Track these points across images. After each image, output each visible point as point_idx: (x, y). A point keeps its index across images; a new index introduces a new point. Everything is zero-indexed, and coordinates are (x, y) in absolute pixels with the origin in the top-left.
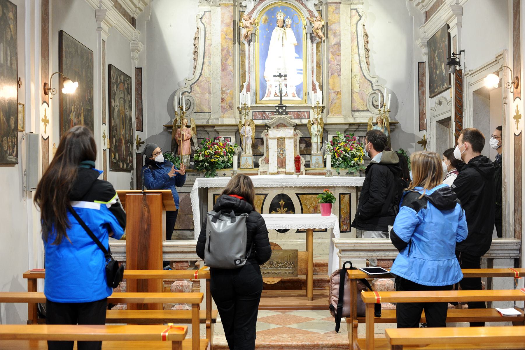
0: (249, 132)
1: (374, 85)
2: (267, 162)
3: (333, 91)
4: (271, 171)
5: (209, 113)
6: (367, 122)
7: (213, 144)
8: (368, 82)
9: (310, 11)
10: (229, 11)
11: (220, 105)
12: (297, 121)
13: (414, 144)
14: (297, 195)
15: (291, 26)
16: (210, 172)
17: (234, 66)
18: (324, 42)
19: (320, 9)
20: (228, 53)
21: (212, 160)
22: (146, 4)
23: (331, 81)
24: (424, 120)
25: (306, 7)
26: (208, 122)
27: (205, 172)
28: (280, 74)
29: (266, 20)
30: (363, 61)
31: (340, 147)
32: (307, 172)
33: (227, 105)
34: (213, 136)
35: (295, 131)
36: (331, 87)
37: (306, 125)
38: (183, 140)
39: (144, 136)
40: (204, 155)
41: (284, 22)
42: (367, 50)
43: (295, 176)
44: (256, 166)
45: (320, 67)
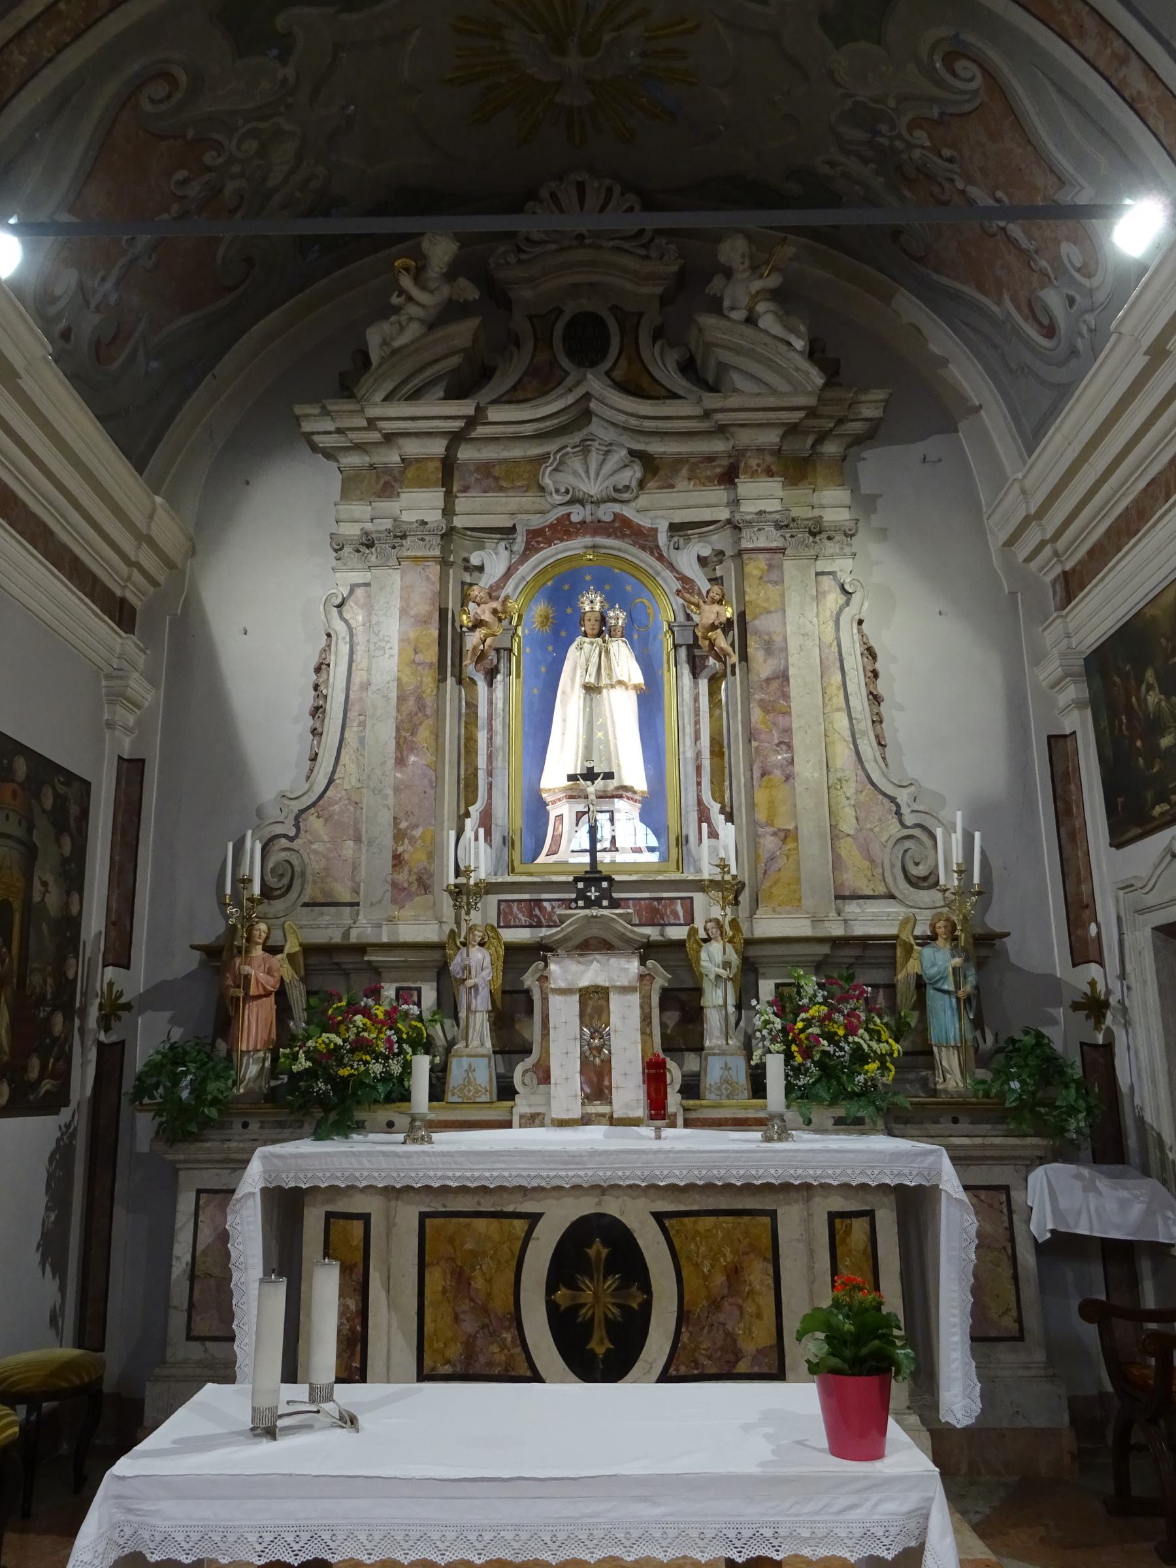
0: (480, 966)
1: (905, 810)
2: (544, 1075)
3: (769, 830)
5: (352, 904)
6: (894, 931)
8: (886, 801)
9: (684, 579)
10: (428, 578)
11: (389, 878)
12: (652, 933)
15: (626, 634)
18: (733, 673)
19: (718, 574)
20: (421, 707)
22: (170, 564)
23: (760, 796)
25: (671, 567)
26: (346, 934)
29: (547, 617)
30: (864, 733)
31: (808, 1023)
32: (693, 1115)
33: (413, 878)
35: (643, 963)
36: (761, 816)
37: (680, 944)
39: (133, 982)
41: (603, 620)
44: (506, 1091)
45: (721, 754)
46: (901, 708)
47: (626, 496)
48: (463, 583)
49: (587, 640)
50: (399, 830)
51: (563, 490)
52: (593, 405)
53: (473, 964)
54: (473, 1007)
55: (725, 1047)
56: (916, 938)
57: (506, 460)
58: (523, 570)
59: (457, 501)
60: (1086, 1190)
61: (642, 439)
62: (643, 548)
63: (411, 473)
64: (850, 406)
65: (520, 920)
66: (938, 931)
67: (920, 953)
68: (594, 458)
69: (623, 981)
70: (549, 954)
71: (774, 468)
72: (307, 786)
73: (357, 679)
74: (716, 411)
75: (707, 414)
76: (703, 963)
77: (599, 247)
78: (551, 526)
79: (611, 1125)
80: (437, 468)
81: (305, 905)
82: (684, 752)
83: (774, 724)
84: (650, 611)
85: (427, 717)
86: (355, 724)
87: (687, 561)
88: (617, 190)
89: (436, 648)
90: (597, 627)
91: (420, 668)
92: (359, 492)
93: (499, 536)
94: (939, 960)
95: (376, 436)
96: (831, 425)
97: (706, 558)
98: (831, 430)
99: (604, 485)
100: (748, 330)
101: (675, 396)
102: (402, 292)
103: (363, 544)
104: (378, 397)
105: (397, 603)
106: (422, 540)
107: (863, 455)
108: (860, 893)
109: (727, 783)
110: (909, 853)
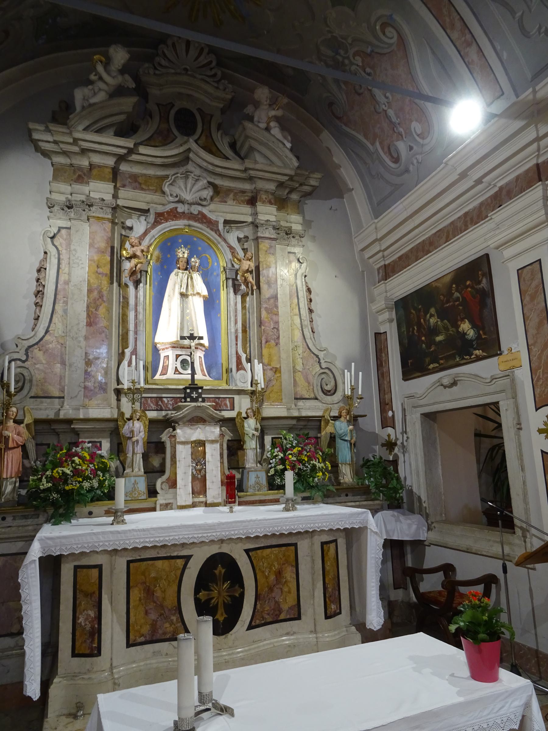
0: (138, 430)
2: (173, 484)
3: (269, 367)
4: (180, 502)
5: (59, 398)
6: (320, 414)
7: (70, 455)
8: (314, 357)
9: (231, 248)
10: (105, 229)
11: (82, 385)
13: (377, 448)
14: (247, 551)
16: (61, 511)
17: (110, 319)
18: (252, 294)
19: (245, 247)
21: (67, 488)
23: (265, 351)
24: (386, 412)
25: (225, 240)
27: (51, 511)
28: (192, 335)
29: (158, 258)
30: (307, 326)
32: (242, 500)
34: (65, 439)
37: (232, 420)
38: (7, 448)
40: (50, 479)
41: (188, 262)
42: (311, 311)
43: (226, 509)
44: (152, 492)
46: (320, 316)
47: (204, 203)
48: (121, 235)
49: (181, 271)
50: (89, 360)
51: (175, 195)
52: (191, 155)
53: (135, 429)
54: (136, 451)
55: (256, 468)
56: (331, 417)
57: (145, 175)
58: (153, 232)
59: (119, 191)
60: (396, 521)
61: (213, 177)
62: (212, 229)
63: (95, 172)
64: (306, 179)
65: (152, 407)
66: (342, 414)
67: (334, 424)
68: (190, 182)
69: (213, 438)
70: (177, 425)
71: (273, 201)
72: (33, 333)
73: (62, 278)
74: (250, 169)
75: (246, 170)
76: (246, 429)
77: (195, 77)
78: (168, 212)
79: (206, 506)
80: (110, 172)
81: (31, 397)
82: (230, 329)
83: (272, 319)
84: (210, 261)
85: (104, 302)
86: (61, 302)
87: (232, 238)
88: (206, 50)
89: (109, 266)
90: (185, 265)
91: (100, 276)
92: (63, 178)
93: (139, 213)
94: (342, 427)
95: (76, 149)
96: (297, 186)
97: (241, 238)
98: (297, 188)
99: (194, 196)
100: (266, 134)
101: (227, 158)
103: (67, 206)
104: (81, 128)
105: (87, 240)
106: (102, 209)
107: (306, 202)
108: (304, 397)
109: (248, 345)
110: (324, 380)
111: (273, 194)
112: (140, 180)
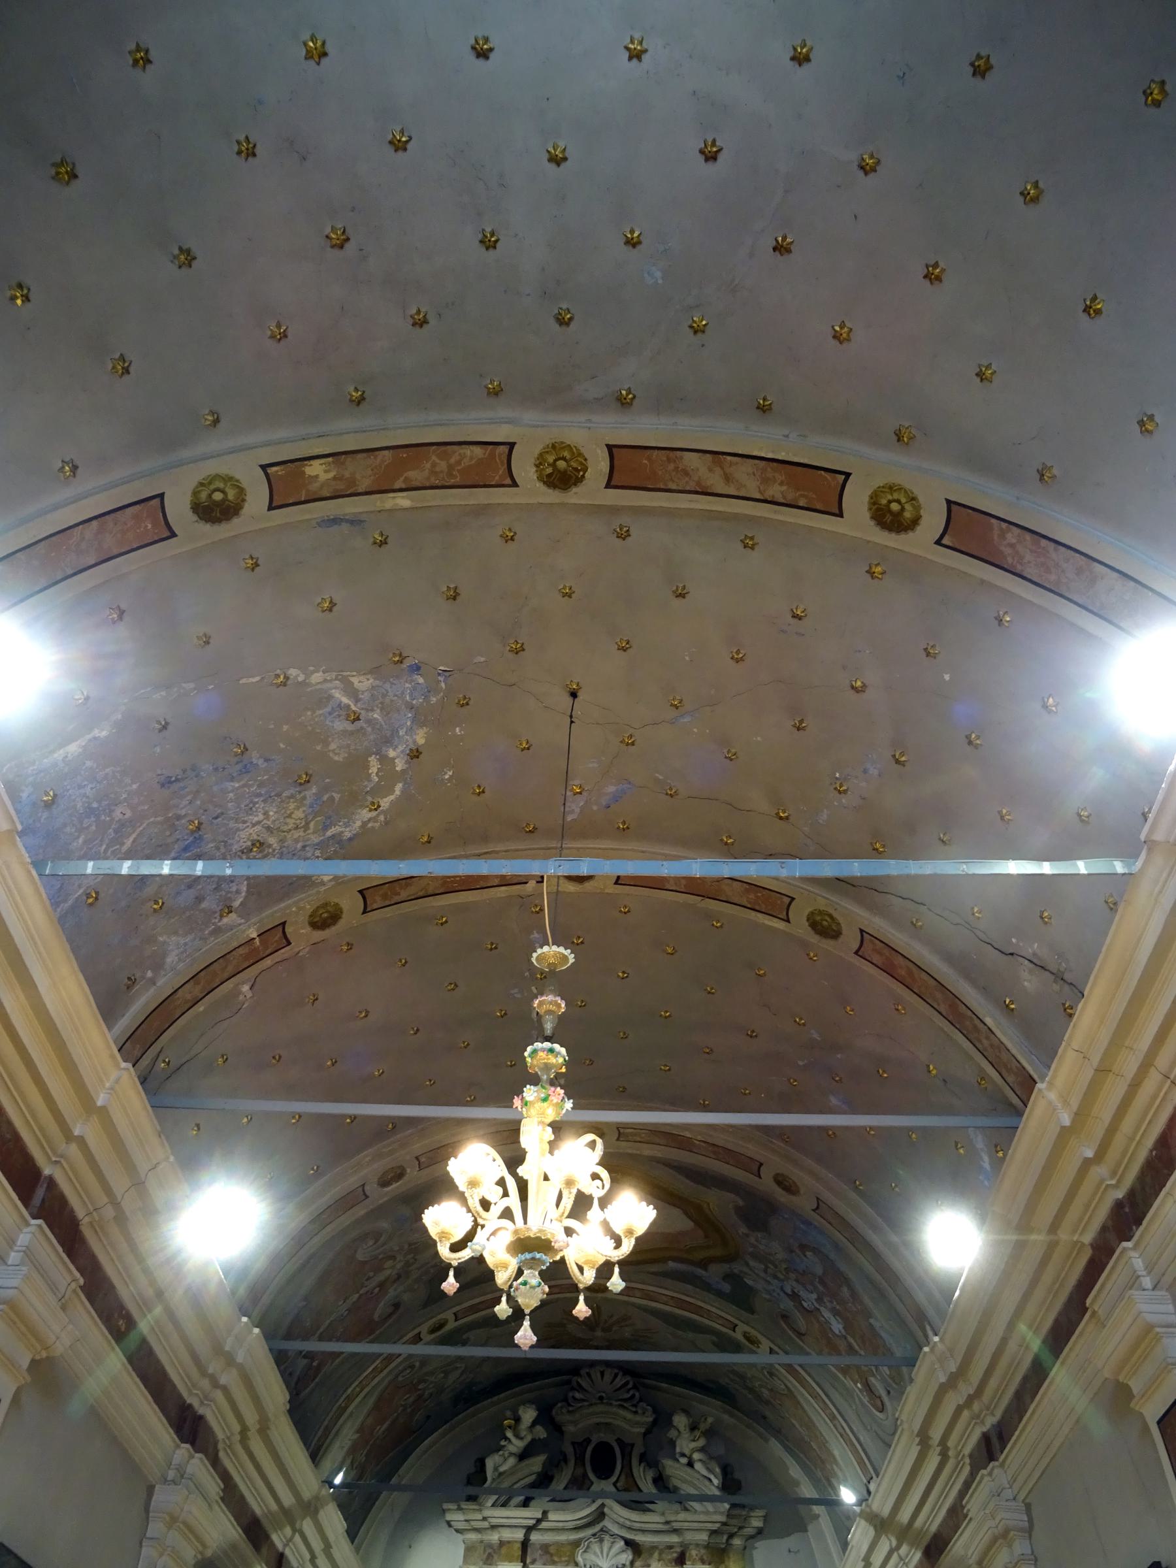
52: (606, 1510)
63: (504, 1550)
68: (606, 1545)
95: (486, 1524)
100: (689, 1470)
102: (506, 1439)
104: (490, 1503)
107: (757, 1545)
111: (707, 1547)
112: (552, 1550)
